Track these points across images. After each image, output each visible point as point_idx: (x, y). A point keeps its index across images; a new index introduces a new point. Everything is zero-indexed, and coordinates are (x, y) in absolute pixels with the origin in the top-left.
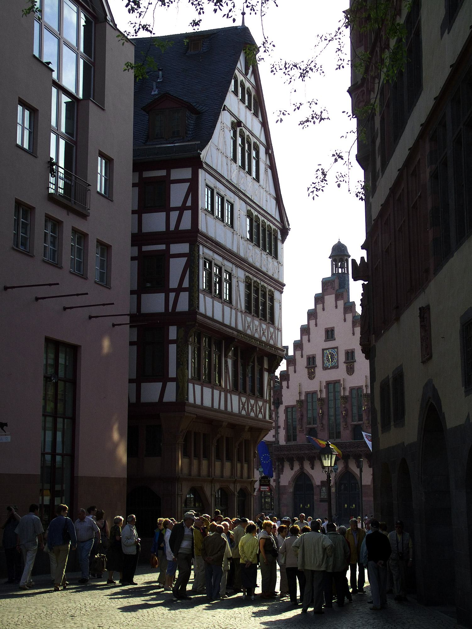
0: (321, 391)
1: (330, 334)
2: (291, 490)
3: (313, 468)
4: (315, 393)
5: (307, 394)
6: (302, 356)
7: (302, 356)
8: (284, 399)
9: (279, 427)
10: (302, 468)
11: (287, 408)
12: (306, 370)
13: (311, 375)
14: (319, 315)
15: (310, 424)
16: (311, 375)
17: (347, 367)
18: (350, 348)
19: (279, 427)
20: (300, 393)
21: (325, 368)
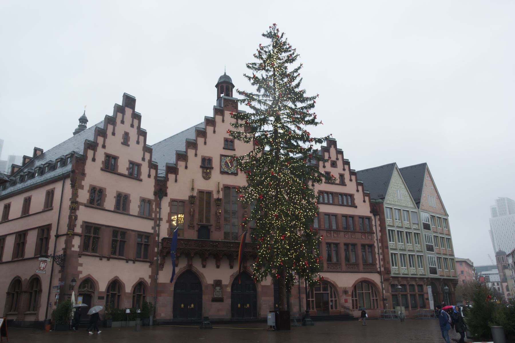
0: (218, 192)
2: (172, 288)
3: (204, 266)
4: (209, 194)
5: (201, 192)
6: (196, 155)
7: (196, 155)
8: (169, 191)
9: (160, 219)
10: (190, 266)
12: (200, 170)
13: (207, 176)
14: (217, 124)
16: (207, 176)
19: (160, 219)
20: (193, 189)
21: (222, 173)
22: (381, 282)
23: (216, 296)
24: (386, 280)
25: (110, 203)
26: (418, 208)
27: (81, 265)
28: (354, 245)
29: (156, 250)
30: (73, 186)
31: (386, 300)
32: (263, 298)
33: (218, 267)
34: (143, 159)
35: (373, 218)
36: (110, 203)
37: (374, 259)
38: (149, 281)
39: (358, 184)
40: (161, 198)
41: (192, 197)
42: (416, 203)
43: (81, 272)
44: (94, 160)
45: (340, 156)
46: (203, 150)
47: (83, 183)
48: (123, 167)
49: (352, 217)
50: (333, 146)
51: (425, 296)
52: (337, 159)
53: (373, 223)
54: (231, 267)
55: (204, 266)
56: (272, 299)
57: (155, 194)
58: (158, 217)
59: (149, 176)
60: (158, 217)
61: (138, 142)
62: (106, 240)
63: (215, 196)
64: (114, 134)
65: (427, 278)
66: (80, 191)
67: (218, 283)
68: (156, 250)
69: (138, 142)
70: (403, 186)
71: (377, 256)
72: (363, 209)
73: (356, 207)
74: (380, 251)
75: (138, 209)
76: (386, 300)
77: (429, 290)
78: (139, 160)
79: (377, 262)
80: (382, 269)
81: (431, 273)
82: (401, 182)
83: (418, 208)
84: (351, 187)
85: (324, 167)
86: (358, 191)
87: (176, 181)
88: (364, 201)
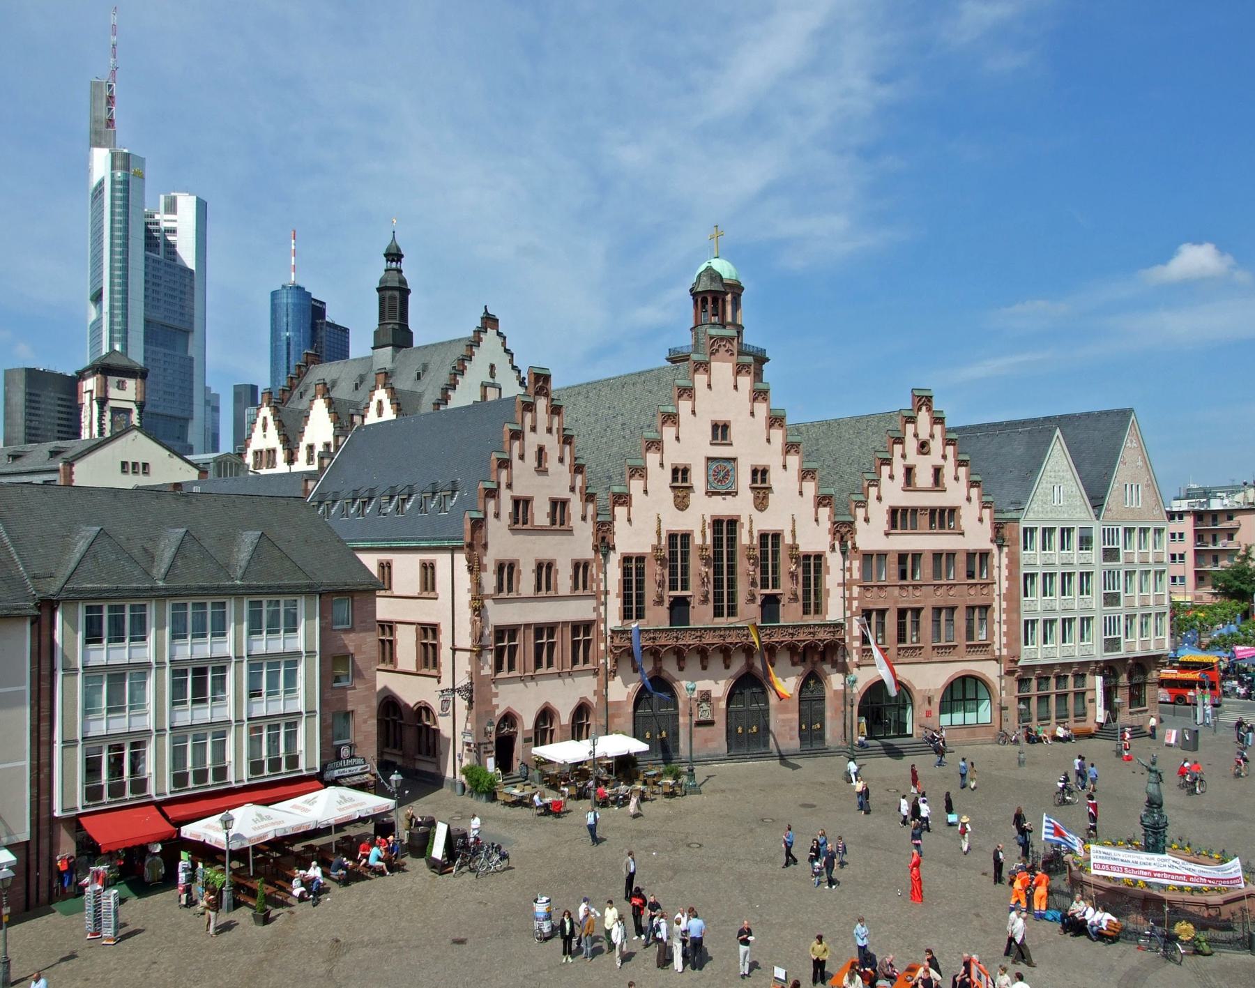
1: (720, 431)
2: (631, 709)
3: (681, 669)
5: (672, 537)
6: (662, 465)
7: (662, 465)
10: (658, 669)
11: (626, 559)
13: (682, 504)
14: (698, 394)
15: (673, 587)
16: (682, 504)
17: (756, 498)
18: (761, 462)
20: (659, 533)
21: (710, 493)
22: (1001, 677)
23: (702, 719)
24: (1010, 673)
25: (526, 583)
26: (1098, 517)
27: (496, 695)
28: (952, 609)
29: (602, 646)
30: (471, 570)
31: (1006, 708)
32: (781, 716)
33: (704, 668)
34: (572, 489)
35: (995, 550)
36: (526, 583)
37: (990, 634)
38: (593, 699)
39: (973, 484)
40: (605, 556)
41: (656, 548)
42: (1094, 507)
43: (497, 706)
44: (497, 515)
45: (938, 429)
46: (674, 454)
47: (485, 560)
48: (540, 514)
49: (951, 555)
50: (924, 408)
51: (1089, 696)
52: (932, 436)
53: (996, 562)
54: (727, 667)
55: (681, 669)
56: (797, 716)
57: (596, 549)
58: (602, 588)
59: (584, 518)
60: (602, 588)
61: (561, 460)
62: (526, 645)
63: (697, 540)
64: (522, 457)
65: (1097, 662)
66: (483, 574)
67: (706, 697)
68: (602, 646)
69: (561, 460)
70: (1069, 475)
71: (996, 627)
72: (975, 533)
73: (962, 534)
74: (1004, 617)
75: (570, 583)
76: (1006, 708)
77: (1097, 683)
78: (565, 494)
79: (996, 639)
80: (1004, 652)
81: (1106, 650)
82: (1066, 467)
83: (1098, 517)
84: (955, 493)
85: (904, 456)
86: (969, 499)
87: (629, 520)
88: (981, 520)
